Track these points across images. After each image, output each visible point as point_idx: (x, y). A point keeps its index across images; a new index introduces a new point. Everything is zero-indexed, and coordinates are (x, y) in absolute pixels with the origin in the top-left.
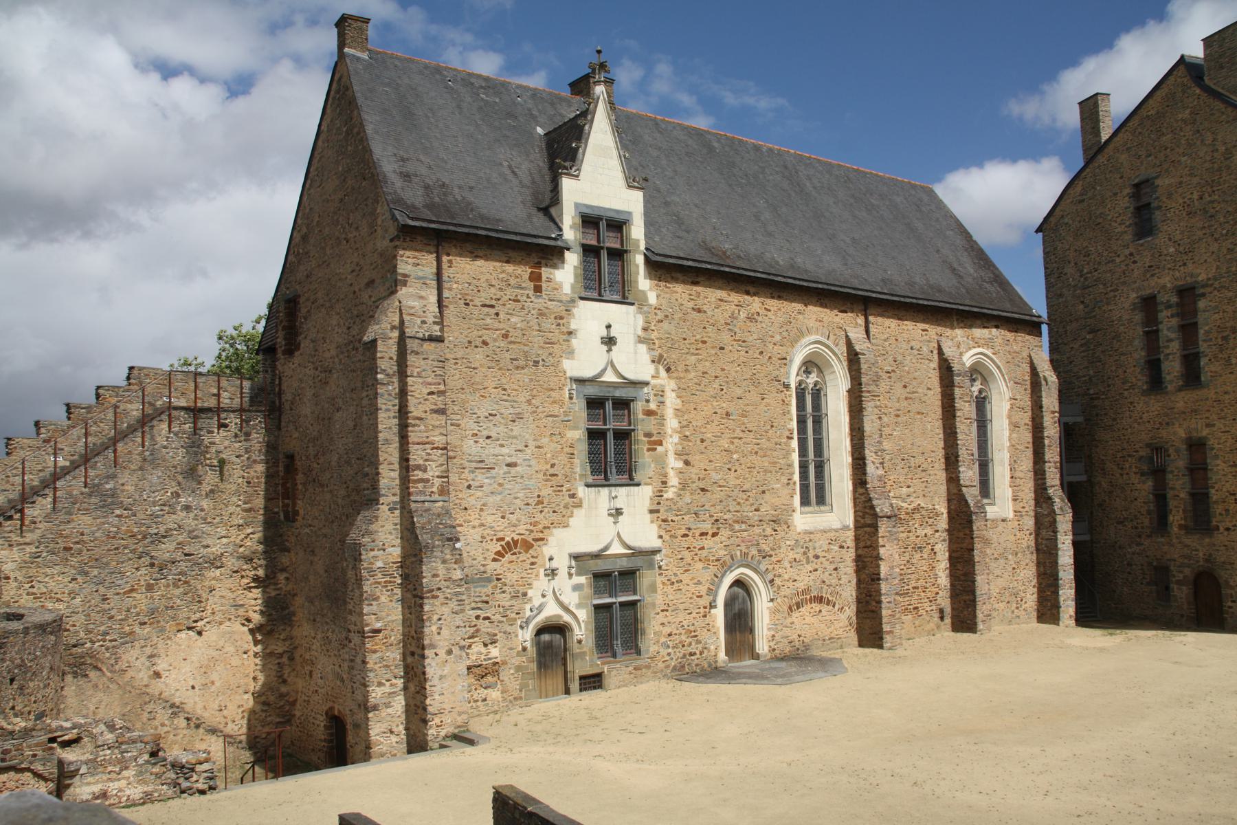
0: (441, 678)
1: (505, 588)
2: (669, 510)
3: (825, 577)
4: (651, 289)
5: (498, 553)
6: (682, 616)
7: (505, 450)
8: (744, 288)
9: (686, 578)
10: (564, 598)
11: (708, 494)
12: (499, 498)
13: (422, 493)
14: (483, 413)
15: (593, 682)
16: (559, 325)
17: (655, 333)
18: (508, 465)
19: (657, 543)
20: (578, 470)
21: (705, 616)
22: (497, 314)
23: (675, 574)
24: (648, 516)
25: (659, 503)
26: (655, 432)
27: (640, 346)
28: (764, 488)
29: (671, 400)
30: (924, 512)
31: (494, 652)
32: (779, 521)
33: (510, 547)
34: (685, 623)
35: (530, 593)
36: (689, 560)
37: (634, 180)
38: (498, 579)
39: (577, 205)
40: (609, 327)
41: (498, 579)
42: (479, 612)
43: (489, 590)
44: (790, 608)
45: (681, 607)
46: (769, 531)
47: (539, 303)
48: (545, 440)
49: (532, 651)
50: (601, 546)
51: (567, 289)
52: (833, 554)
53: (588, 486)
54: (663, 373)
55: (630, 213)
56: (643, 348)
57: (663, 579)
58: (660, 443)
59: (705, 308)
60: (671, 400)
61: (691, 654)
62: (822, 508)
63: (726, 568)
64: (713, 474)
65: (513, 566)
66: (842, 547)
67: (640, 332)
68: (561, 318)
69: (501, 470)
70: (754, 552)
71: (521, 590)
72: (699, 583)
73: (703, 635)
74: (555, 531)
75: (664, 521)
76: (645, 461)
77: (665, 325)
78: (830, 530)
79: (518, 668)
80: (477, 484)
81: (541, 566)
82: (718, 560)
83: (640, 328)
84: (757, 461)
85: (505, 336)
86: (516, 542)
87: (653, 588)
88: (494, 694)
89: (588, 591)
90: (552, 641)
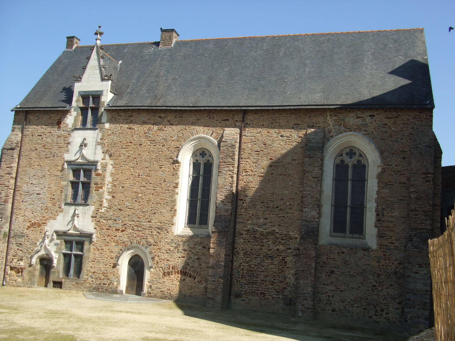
1: (29, 240)
5: (28, 226)
6: (101, 265)
7: (37, 189)
8: (158, 115)
9: (106, 248)
11: (122, 212)
12: (32, 206)
15: (58, 284)
16: (65, 140)
17: (106, 140)
22: (42, 138)
24: (91, 219)
25: (97, 214)
26: (100, 183)
27: (98, 146)
29: (110, 168)
30: (278, 235)
33: (33, 225)
36: (108, 240)
38: (27, 236)
39: (79, 92)
42: (19, 248)
43: (23, 240)
45: (101, 261)
46: (155, 233)
48: (52, 185)
52: (197, 250)
54: (107, 157)
55: (102, 91)
56: (99, 147)
58: (102, 188)
60: (110, 168)
61: (104, 284)
62: (203, 226)
65: (33, 232)
67: (99, 141)
68: (66, 138)
70: (144, 241)
72: (112, 252)
73: (111, 276)
74: (51, 221)
80: (25, 200)
83: (99, 138)
85: (44, 146)
86: (35, 223)
87: (89, 250)
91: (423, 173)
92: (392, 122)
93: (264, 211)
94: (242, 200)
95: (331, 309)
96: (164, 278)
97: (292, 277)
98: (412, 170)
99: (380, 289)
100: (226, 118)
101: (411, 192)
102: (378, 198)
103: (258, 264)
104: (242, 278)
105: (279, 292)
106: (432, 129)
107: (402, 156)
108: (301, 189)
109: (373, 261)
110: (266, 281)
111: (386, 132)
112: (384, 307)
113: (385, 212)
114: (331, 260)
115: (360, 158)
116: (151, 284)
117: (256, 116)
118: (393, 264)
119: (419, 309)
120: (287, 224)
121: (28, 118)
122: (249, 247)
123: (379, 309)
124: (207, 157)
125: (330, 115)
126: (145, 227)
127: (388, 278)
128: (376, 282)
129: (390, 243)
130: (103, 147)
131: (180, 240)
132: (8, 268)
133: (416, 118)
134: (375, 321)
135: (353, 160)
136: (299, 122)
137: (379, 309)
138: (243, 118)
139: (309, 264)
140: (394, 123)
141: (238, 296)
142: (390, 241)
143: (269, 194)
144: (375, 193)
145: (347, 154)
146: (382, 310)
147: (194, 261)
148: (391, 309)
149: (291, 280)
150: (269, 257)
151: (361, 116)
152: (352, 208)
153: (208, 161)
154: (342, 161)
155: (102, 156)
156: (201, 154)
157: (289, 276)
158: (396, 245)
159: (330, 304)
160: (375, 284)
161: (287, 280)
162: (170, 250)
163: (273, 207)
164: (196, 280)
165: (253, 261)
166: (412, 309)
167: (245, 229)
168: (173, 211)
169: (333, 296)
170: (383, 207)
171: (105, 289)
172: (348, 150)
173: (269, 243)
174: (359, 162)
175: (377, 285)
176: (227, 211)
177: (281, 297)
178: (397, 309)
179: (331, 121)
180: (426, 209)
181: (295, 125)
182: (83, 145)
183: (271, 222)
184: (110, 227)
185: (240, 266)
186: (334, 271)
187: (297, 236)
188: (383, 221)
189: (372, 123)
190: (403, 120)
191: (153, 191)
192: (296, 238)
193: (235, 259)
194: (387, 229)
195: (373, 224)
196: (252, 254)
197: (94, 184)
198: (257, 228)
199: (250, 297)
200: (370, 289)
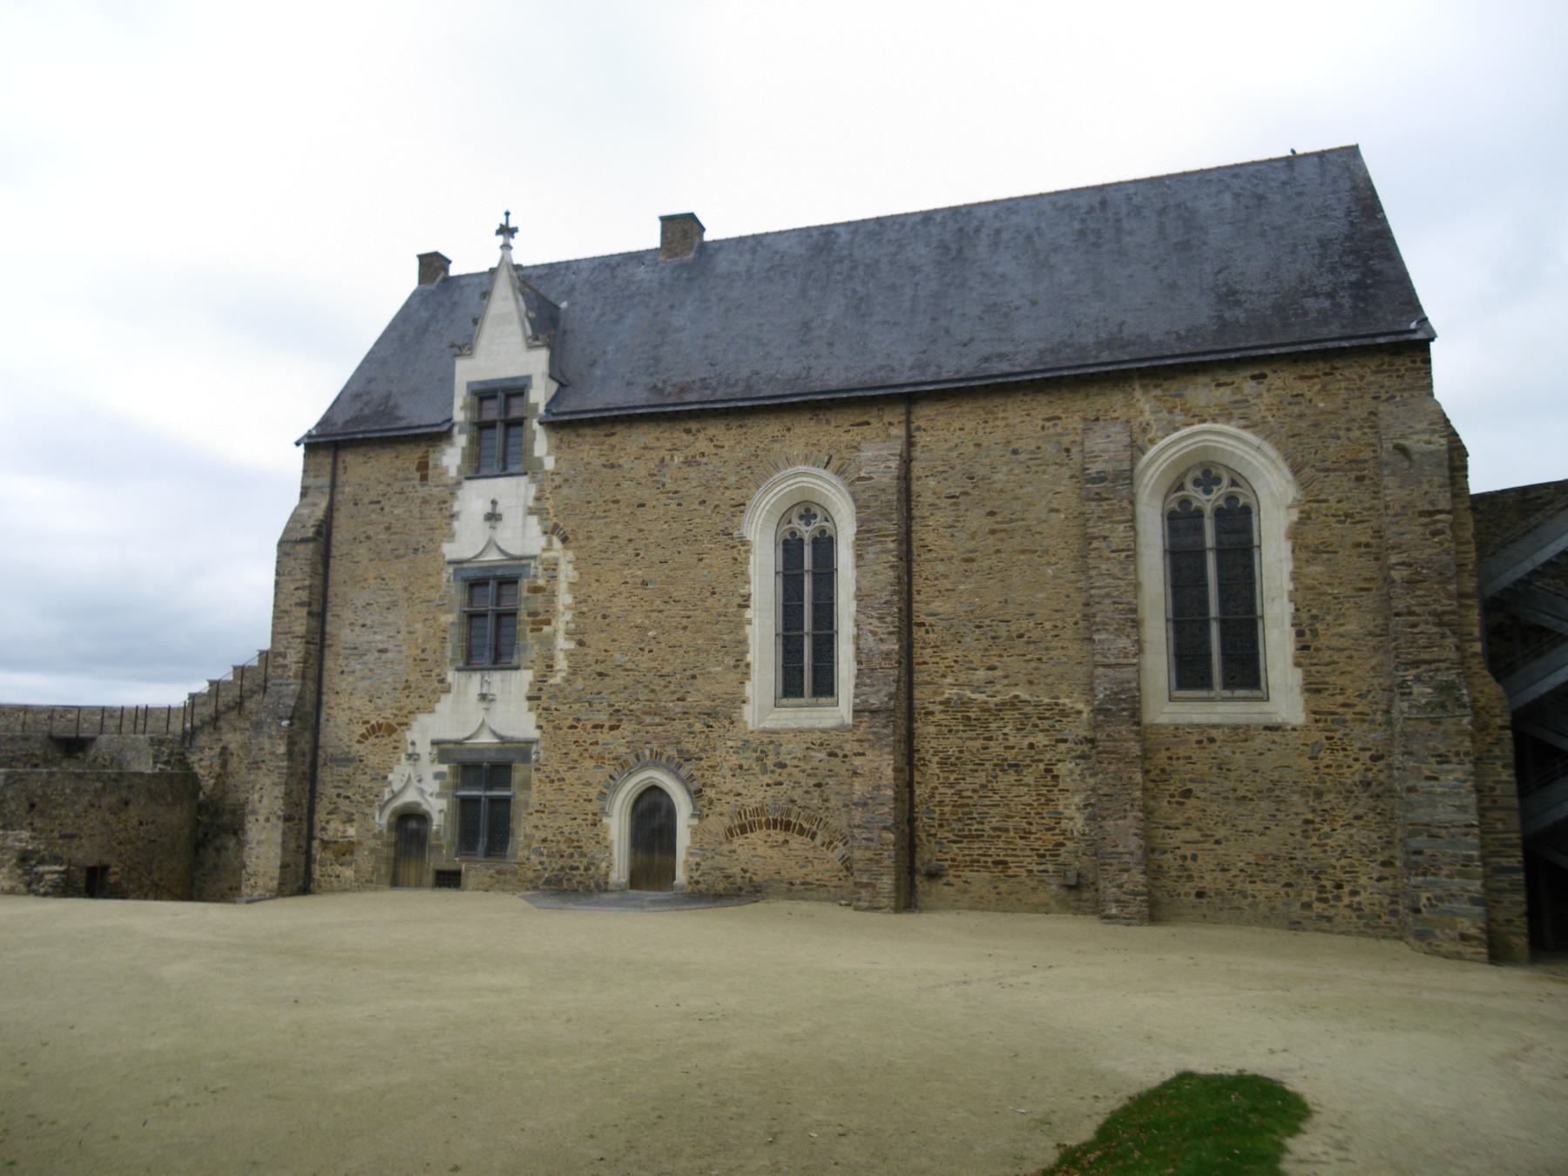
0: (259, 843)
2: (553, 697)
3: (797, 794)
4: (548, 454)
5: (363, 736)
7: (378, 637)
8: (684, 425)
10: (425, 788)
11: (607, 679)
12: (367, 683)
13: (281, 677)
14: (360, 602)
15: (449, 879)
18: (380, 651)
19: (536, 734)
20: (449, 654)
21: (594, 825)
23: (557, 772)
24: (526, 704)
26: (541, 610)
28: (696, 672)
29: (567, 573)
30: (1028, 709)
31: (351, 831)
32: (723, 712)
33: (374, 730)
34: (566, 830)
35: (391, 777)
36: (575, 756)
37: (532, 342)
40: (494, 503)
43: (350, 770)
44: (730, 830)
46: (698, 726)
47: (423, 491)
48: (418, 626)
50: (467, 734)
51: (453, 472)
52: (815, 763)
53: (459, 670)
55: (529, 378)
56: (534, 520)
57: (541, 775)
58: (548, 623)
59: (621, 461)
60: (567, 573)
61: (573, 868)
62: (822, 700)
63: (626, 767)
64: (617, 656)
66: (832, 754)
67: (531, 503)
69: (371, 657)
70: (671, 751)
71: (382, 773)
72: (588, 784)
73: (590, 848)
75: (546, 709)
76: (529, 641)
77: (565, 491)
78: (811, 730)
79: (372, 851)
82: (615, 759)
84: (684, 638)
85: (388, 529)
86: (380, 726)
87: (527, 785)
88: (348, 873)
89: (449, 779)
90: (410, 823)
91: (1422, 514)
92: (1317, 387)
93: (986, 650)
94: (923, 624)
95: (1193, 892)
96: (731, 842)
97: (1077, 815)
98: (1387, 507)
99: (1326, 828)
100: (861, 420)
101: (1392, 567)
102: (1296, 589)
103: (983, 786)
104: (941, 826)
105: (1043, 856)
106: (1432, 395)
107: (1353, 474)
108: (1079, 585)
109: (1300, 756)
110: (1007, 830)
111: (1301, 416)
112: (1344, 877)
113: (1319, 627)
114: (1182, 762)
115: (1234, 489)
116: (698, 859)
117: (942, 407)
118: (1356, 760)
119: (1450, 876)
120: (1049, 680)
121: (340, 461)
122: (951, 745)
123: (1329, 884)
124: (818, 523)
125: (1144, 387)
126: (671, 714)
127: (1347, 799)
128: (1314, 811)
129: (1344, 705)
130: (542, 520)
131: (766, 741)
132: (316, 844)
133: (1383, 372)
134: (1320, 917)
135: (1213, 496)
136: (1058, 413)
137: (1329, 884)
138: (909, 413)
139: (1125, 775)
140: (1323, 388)
141: (934, 875)
142: (1340, 699)
143: (996, 605)
144: (1286, 577)
145: (1197, 483)
146: (1339, 886)
147: (807, 792)
148: (1363, 880)
149: (1077, 822)
150: (1010, 766)
151: (1229, 380)
152: (1223, 623)
153: (823, 532)
154: (1185, 502)
155: (543, 541)
156: (801, 517)
157: (1067, 813)
158: (1357, 709)
159: (1190, 878)
160: (1310, 817)
161: (1064, 824)
162: (741, 767)
163: (1010, 638)
164: (818, 840)
165: (969, 780)
166: (1430, 878)
167: (938, 699)
168: (742, 668)
169: (1194, 858)
170: (1314, 611)
171: (570, 884)
172: (1198, 474)
173: (1006, 730)
174: (1231, 498)
175: (1318, 819)
176: (887, 655)
177: (1050, 867)
178: (1380, 879)
179: (1148, 401)
180: (1440, 609)
181: (1048, 420)
182: (493, 517)
183: (1006, 677)
184: (578, 720)
185: (932, 796)
186: (1190, 791)
187: (1080, 706)
188: (1317, 650)
189: (1259, 396)
190: (1348, 379)
191: (685, 621)
192: (1079, 712)
193: (917, 777)
194: (1329, 669)
195: (1290, 660)
196: (964, 763)
197: (529, 615)
198: (968, 693)
199: (967, 874)
200: (1298, 832)
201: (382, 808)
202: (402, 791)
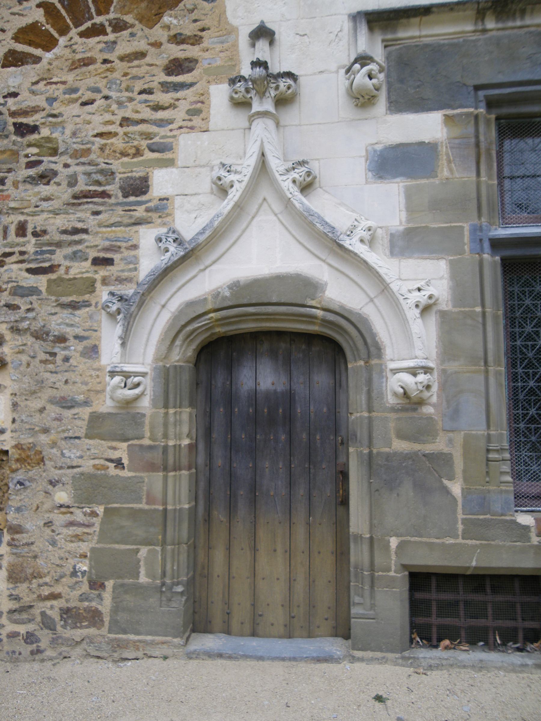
1: (48, 163)
35: (162, 182)
38: (23, 130)
41: (23, 130)
49: (181, 428)
65: (88, 80)
79: (90, 488)
81: (215, 75)
89: (455, 174)
201: (129, 311)
202: (216, 236)
